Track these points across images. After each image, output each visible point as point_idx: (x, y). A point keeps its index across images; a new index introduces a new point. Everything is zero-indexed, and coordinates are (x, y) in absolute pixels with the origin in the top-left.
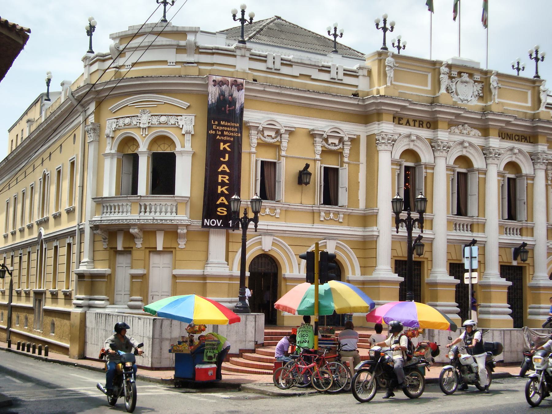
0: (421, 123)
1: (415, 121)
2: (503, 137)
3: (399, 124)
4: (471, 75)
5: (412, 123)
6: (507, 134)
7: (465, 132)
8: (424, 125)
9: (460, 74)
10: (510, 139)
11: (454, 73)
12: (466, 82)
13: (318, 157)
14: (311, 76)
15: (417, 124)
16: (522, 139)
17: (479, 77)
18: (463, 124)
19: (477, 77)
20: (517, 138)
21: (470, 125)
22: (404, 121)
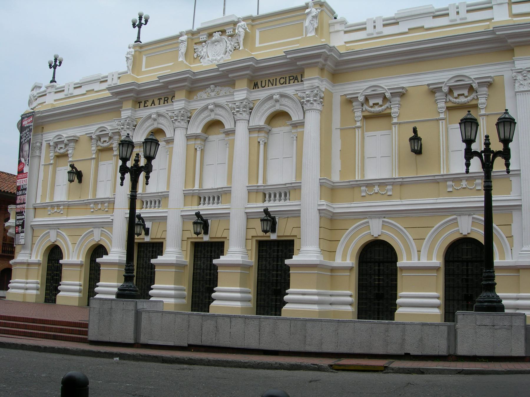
0: (166, 99)
1: (160, 99)
2: (263, 85)
3: (145, 107)
4: (223, 32)
5: (156, 102)
6: (269, 80)
7: (213, 94)
8: (169, 100)
9: (210, 35)
10: (273, 85)
11: (203, 37)
12: (218, 41)
13: (94, 156)
14: (93, 90)
15: (162, 101)
16: (290, 80)
17: (232, 30)
18: (208, 86)
19: (229, 31)
20: (282, 81)
21: (216, 85)
22: (149, 103)
